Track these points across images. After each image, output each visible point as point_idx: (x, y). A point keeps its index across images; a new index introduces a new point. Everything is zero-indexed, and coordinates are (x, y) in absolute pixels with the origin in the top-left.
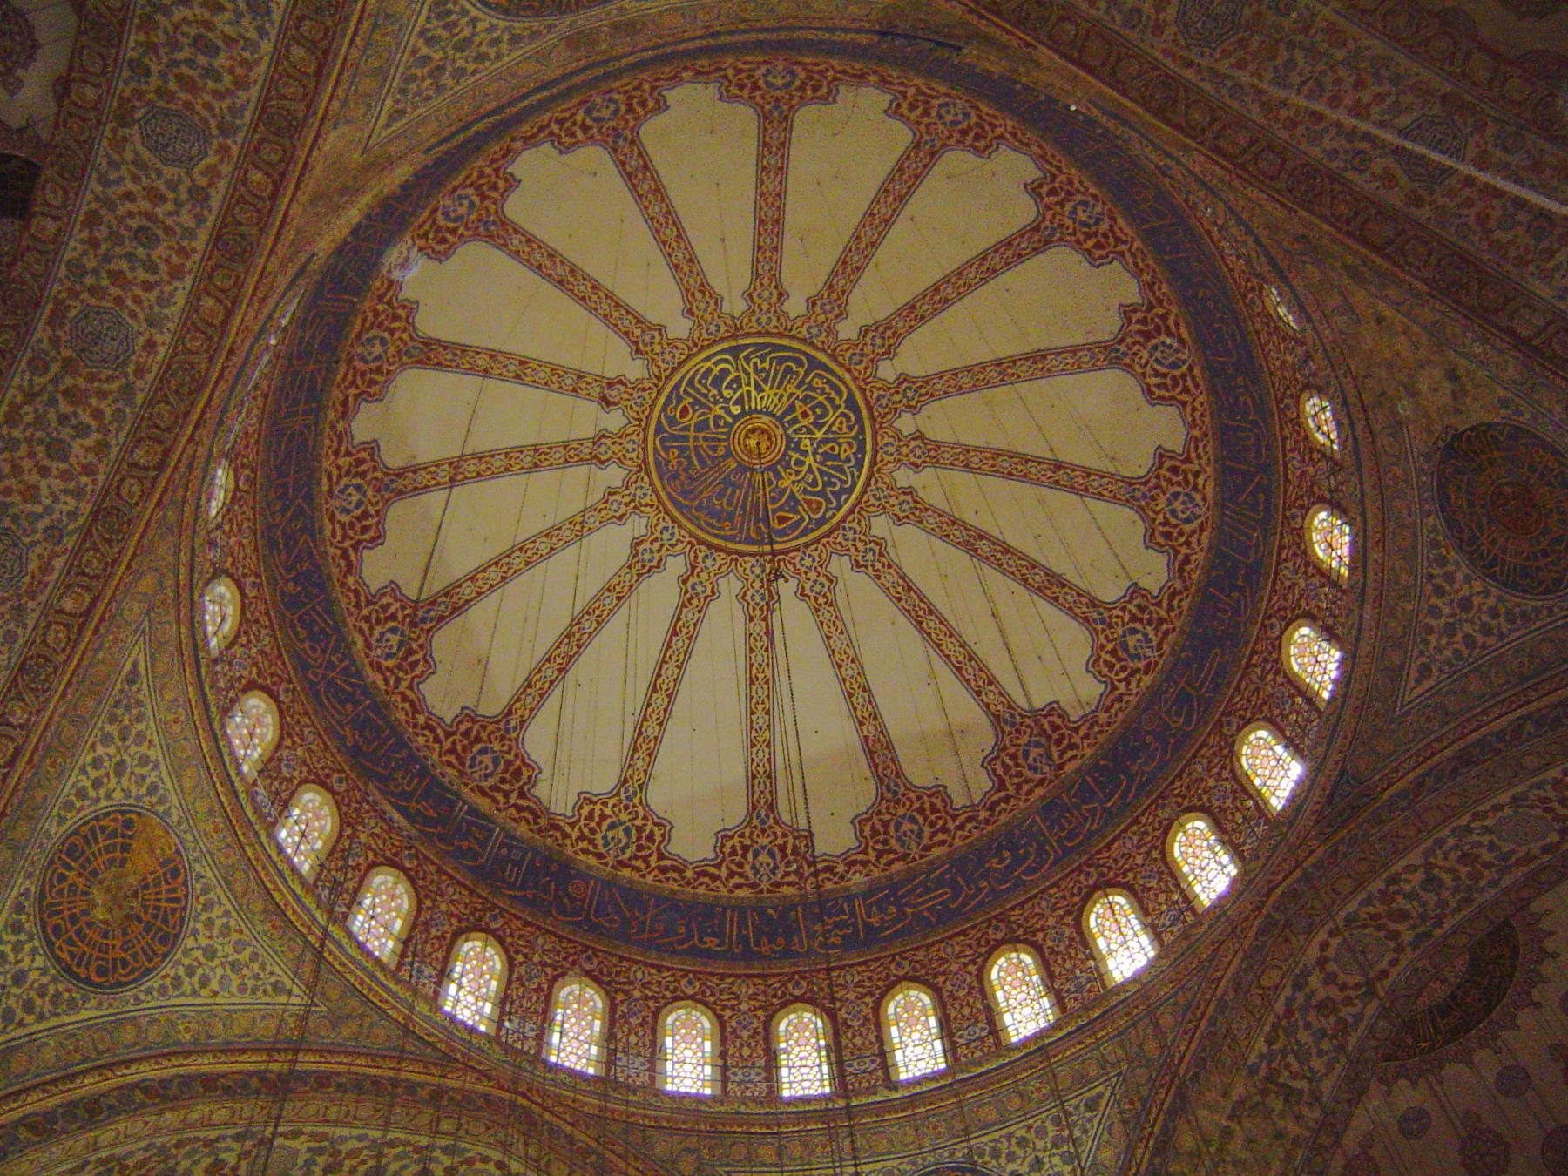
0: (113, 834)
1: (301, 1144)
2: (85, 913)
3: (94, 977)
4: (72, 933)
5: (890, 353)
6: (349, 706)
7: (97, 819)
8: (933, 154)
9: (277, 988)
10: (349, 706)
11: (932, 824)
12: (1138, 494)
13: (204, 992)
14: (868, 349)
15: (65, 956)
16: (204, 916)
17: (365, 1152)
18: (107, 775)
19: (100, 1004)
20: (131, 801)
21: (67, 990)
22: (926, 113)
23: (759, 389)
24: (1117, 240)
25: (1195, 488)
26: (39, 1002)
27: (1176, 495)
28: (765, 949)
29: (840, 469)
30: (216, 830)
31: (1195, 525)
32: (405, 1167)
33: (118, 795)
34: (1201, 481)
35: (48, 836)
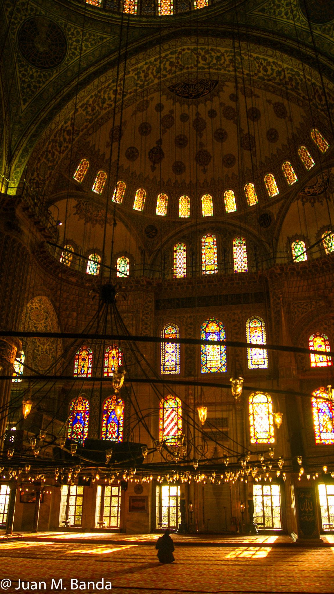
1: (132, 74)
3: (51, 66)
9: (102, 39)
13: (82, 52)
15: (40, 65)
16: (70, 33)
17: (151, 66)
18: (16, 14)
19: (57, 70)
20: (28, 17)
21: (47, 72)
26: (41, 79)
30: (57, 9)
32: (165, 64)
33: (23, 17)
35: (13, 39)
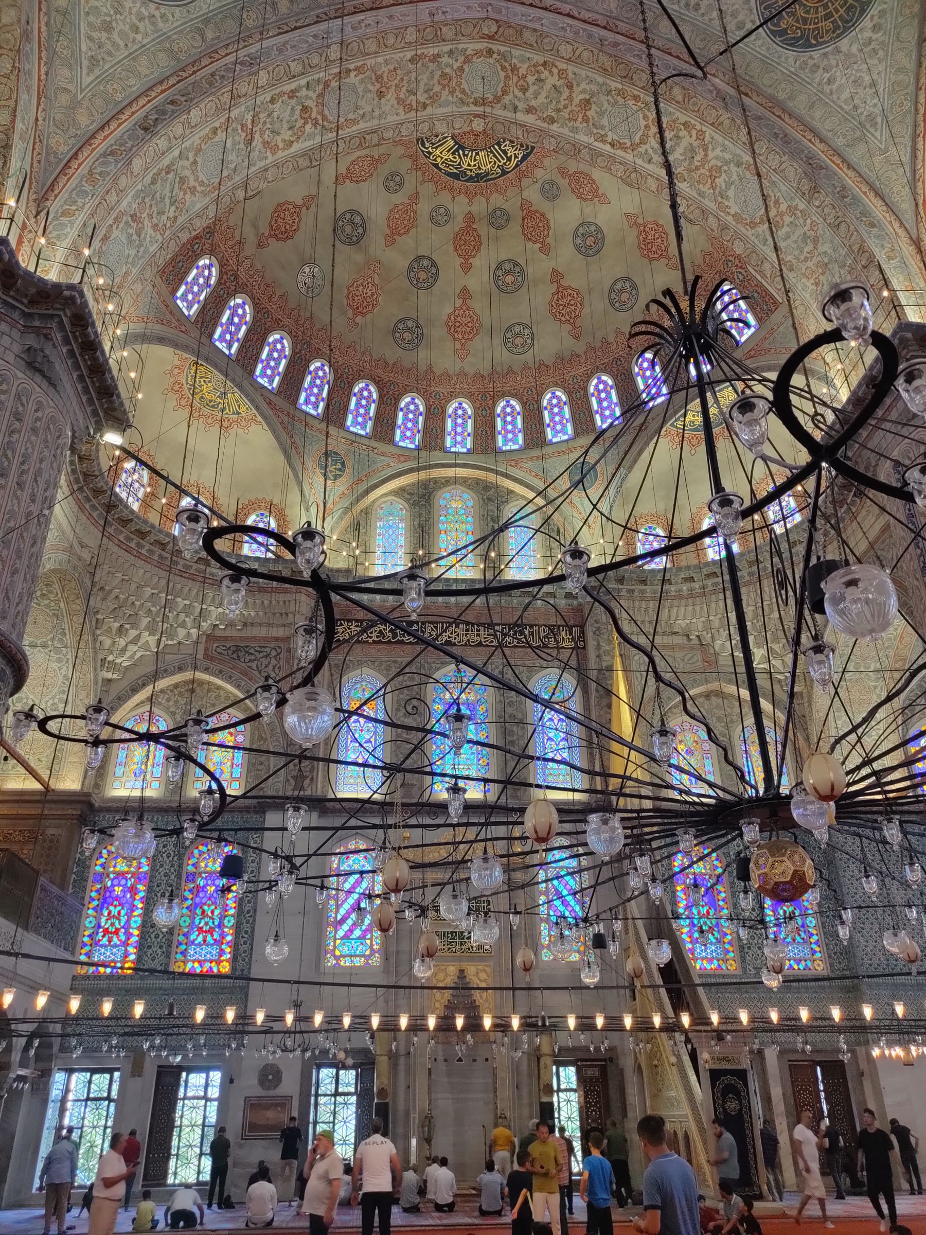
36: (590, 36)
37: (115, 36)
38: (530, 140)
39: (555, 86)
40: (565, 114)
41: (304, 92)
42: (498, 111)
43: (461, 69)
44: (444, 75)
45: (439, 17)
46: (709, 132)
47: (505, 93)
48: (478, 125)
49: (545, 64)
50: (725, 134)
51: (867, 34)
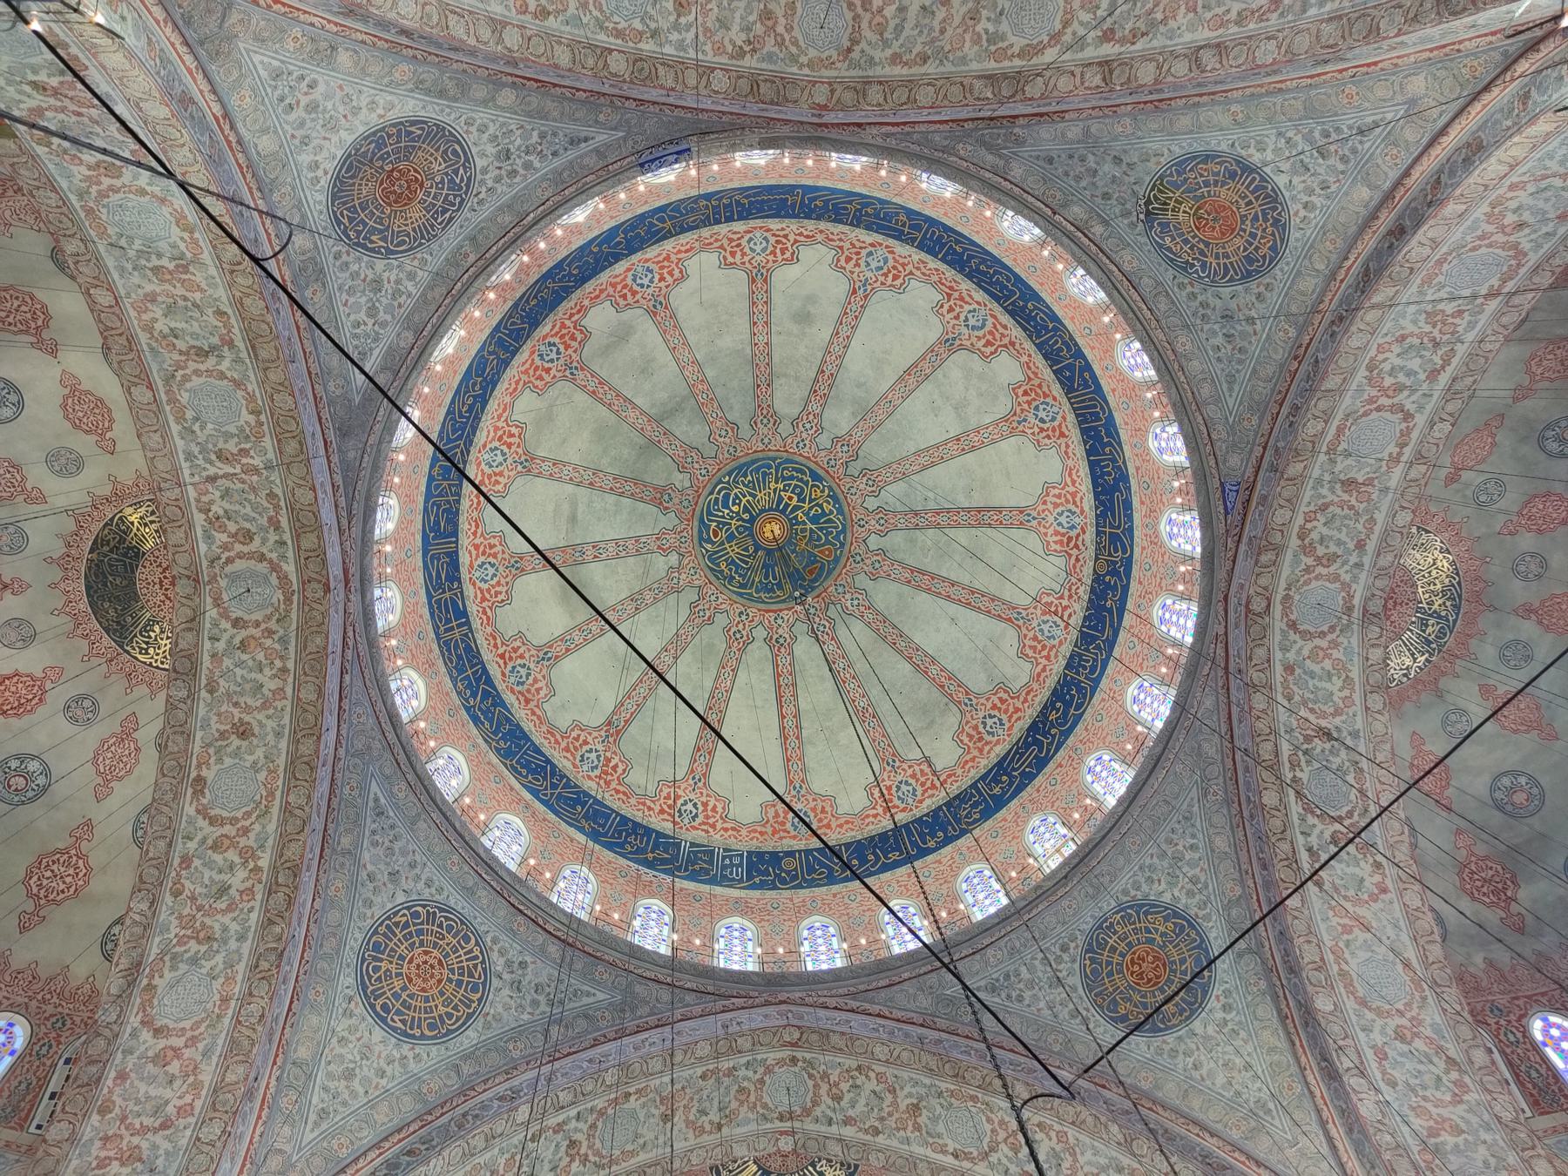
0: (406, 925)
2: (404, 989)
3: (427, 1033)
4: (398, 1005)
5: (820, 429)
6: (579, 808)
7: (389, 918)
8: (765, 281)
10: (579, 808)
11: (1006, 711)
12: (1015, 424)
14: (804, 435)
22: (744, 254)
23: (754, 496)
24: (903, 265)
25: (1046, 396)
27: (1037, 408)
28: (931, 844)
29: (830, 521)
31: (1059, 417)
34: (1045, 389)
36: (907, 1035)
37: (356, 1084)
38: (852, 1158)
39: (874, 1092)
40: (891, 1122)
41: (573, 1124)
42: (809, 1125)
43: (762, 1081)
44: (741, 1090)
45: (734, 1028)
46: (1072, 1133)
47: (815, 1103)
48: (786, 1144)
49: (859, 1068)
50: (1092, 1134)
51: (1220, 1015)
